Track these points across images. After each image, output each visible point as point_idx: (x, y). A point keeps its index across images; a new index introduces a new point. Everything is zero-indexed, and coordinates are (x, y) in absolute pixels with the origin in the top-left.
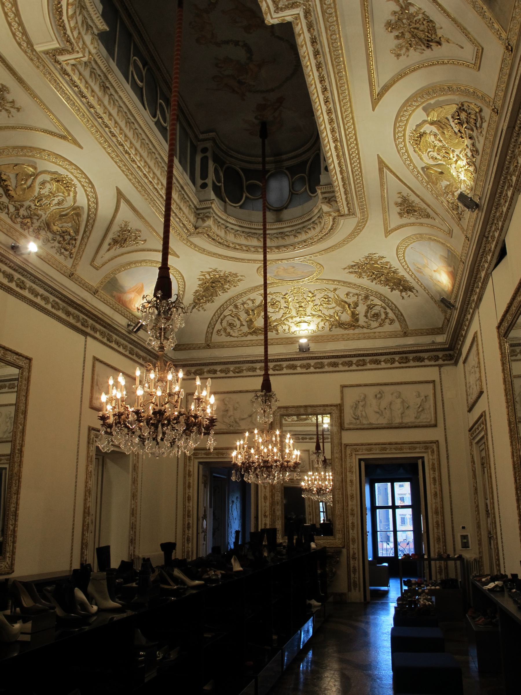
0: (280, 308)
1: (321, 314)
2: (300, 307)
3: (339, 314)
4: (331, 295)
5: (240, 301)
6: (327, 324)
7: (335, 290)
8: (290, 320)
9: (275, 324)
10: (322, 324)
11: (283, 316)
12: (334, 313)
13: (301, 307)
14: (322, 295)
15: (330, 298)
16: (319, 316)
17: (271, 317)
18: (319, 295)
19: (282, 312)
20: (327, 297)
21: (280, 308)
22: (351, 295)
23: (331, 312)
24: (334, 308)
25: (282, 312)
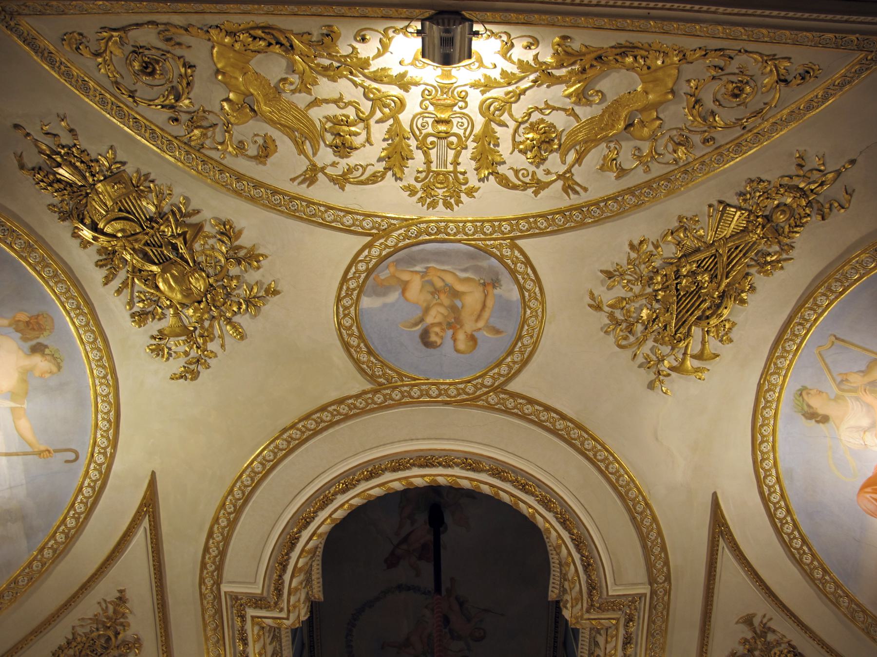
0: (521, 123)
1: (368, 83)
2: (447, 122)
3: (295, 78)
4: (325, 156)
5: (657, 170)
6: (344, 49)
7: (311, 176)
8: (496, 74)
9: (563, 72)
10: (366, 50)
11: (524, 92)
12: (315, 83)
13: (439, 121)
14: (354, 159)
15: (331, 146)
16: (377, 78)
17: (569, 96)
18: (369, 155)
19: (519, 110)
20: (343, 148)
21: (521, 123)
22: (252, 151)
23: (325, 88)
24: (316, 102)
25: (519, 110)
